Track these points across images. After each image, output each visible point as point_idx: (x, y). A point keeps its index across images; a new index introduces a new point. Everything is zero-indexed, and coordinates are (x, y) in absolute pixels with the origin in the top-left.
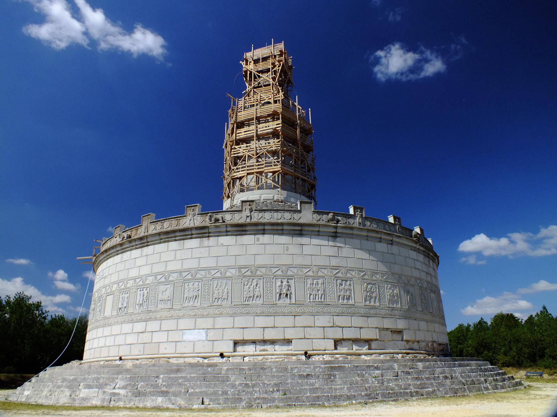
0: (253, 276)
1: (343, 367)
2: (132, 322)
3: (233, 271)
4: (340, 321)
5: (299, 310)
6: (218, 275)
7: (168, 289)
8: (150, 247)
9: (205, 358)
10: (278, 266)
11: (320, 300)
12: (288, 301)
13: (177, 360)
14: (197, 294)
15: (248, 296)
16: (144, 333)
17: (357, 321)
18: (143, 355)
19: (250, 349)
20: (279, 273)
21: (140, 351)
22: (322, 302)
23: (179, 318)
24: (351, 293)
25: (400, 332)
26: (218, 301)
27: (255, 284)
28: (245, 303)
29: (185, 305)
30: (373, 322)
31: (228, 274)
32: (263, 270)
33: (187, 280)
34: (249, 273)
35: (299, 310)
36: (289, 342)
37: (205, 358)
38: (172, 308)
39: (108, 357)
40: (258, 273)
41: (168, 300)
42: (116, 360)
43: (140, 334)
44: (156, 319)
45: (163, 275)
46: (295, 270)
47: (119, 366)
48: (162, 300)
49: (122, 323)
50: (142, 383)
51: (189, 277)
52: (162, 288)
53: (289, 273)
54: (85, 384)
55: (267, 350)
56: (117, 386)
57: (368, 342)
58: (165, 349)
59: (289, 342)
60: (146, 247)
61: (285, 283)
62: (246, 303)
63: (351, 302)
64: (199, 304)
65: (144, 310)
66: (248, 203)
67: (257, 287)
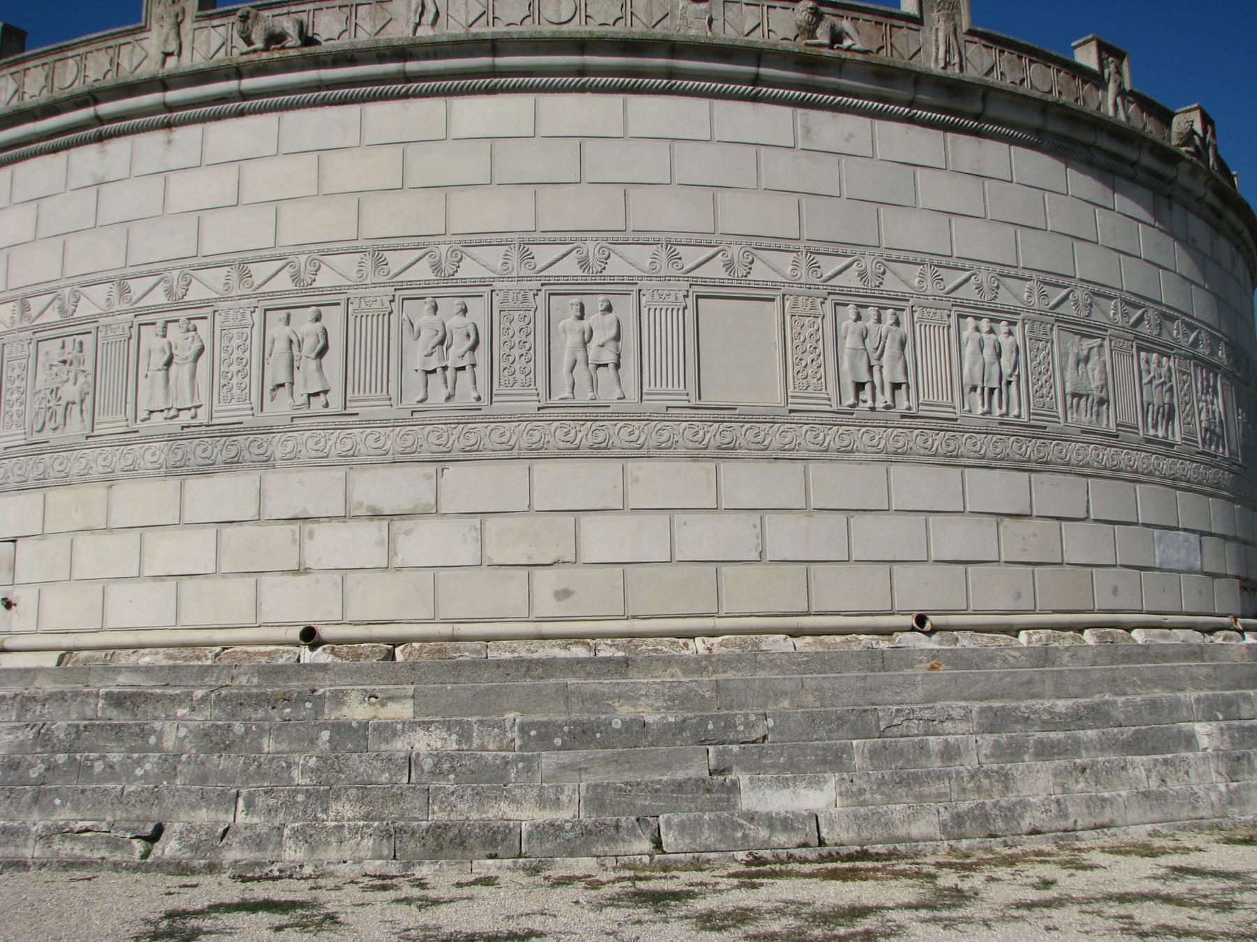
2: (957, 461)
7: (1094, 359)
8: (988, 143)
13: (1163, 636)
16: (1025, 520)
18: (1033, 612)
21: (1019, 595)
38: (1117, 436)
39: (808, 614)
41: (1102, 402)
42: (887, 632)
43: (1007, 521)
44: (1065, 468)
47: (1202, 653)
48: (1080, 396)
49: (890, 457)
54: (1230, 728)
58: (1115, 591)
60: (968, 137)
64: (1178, 438)
65: (1011, 418)
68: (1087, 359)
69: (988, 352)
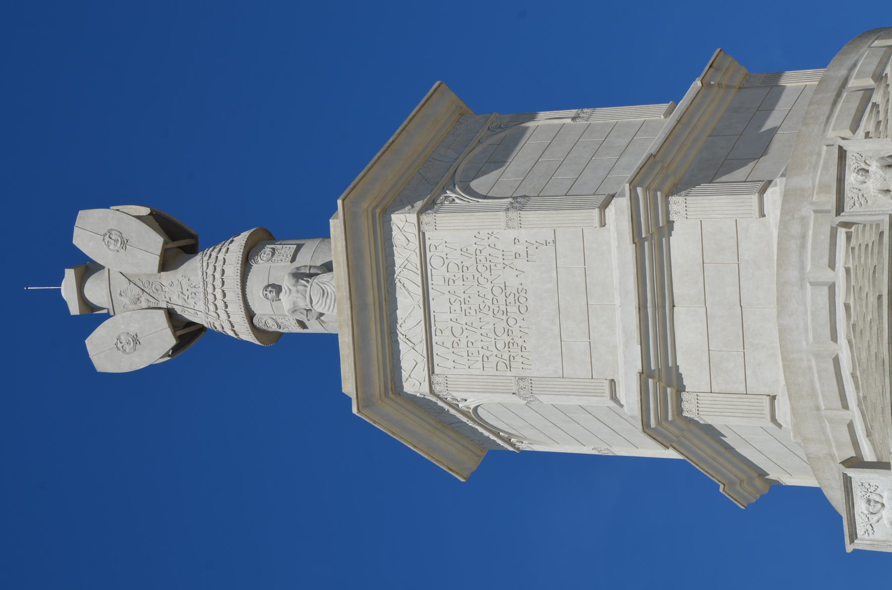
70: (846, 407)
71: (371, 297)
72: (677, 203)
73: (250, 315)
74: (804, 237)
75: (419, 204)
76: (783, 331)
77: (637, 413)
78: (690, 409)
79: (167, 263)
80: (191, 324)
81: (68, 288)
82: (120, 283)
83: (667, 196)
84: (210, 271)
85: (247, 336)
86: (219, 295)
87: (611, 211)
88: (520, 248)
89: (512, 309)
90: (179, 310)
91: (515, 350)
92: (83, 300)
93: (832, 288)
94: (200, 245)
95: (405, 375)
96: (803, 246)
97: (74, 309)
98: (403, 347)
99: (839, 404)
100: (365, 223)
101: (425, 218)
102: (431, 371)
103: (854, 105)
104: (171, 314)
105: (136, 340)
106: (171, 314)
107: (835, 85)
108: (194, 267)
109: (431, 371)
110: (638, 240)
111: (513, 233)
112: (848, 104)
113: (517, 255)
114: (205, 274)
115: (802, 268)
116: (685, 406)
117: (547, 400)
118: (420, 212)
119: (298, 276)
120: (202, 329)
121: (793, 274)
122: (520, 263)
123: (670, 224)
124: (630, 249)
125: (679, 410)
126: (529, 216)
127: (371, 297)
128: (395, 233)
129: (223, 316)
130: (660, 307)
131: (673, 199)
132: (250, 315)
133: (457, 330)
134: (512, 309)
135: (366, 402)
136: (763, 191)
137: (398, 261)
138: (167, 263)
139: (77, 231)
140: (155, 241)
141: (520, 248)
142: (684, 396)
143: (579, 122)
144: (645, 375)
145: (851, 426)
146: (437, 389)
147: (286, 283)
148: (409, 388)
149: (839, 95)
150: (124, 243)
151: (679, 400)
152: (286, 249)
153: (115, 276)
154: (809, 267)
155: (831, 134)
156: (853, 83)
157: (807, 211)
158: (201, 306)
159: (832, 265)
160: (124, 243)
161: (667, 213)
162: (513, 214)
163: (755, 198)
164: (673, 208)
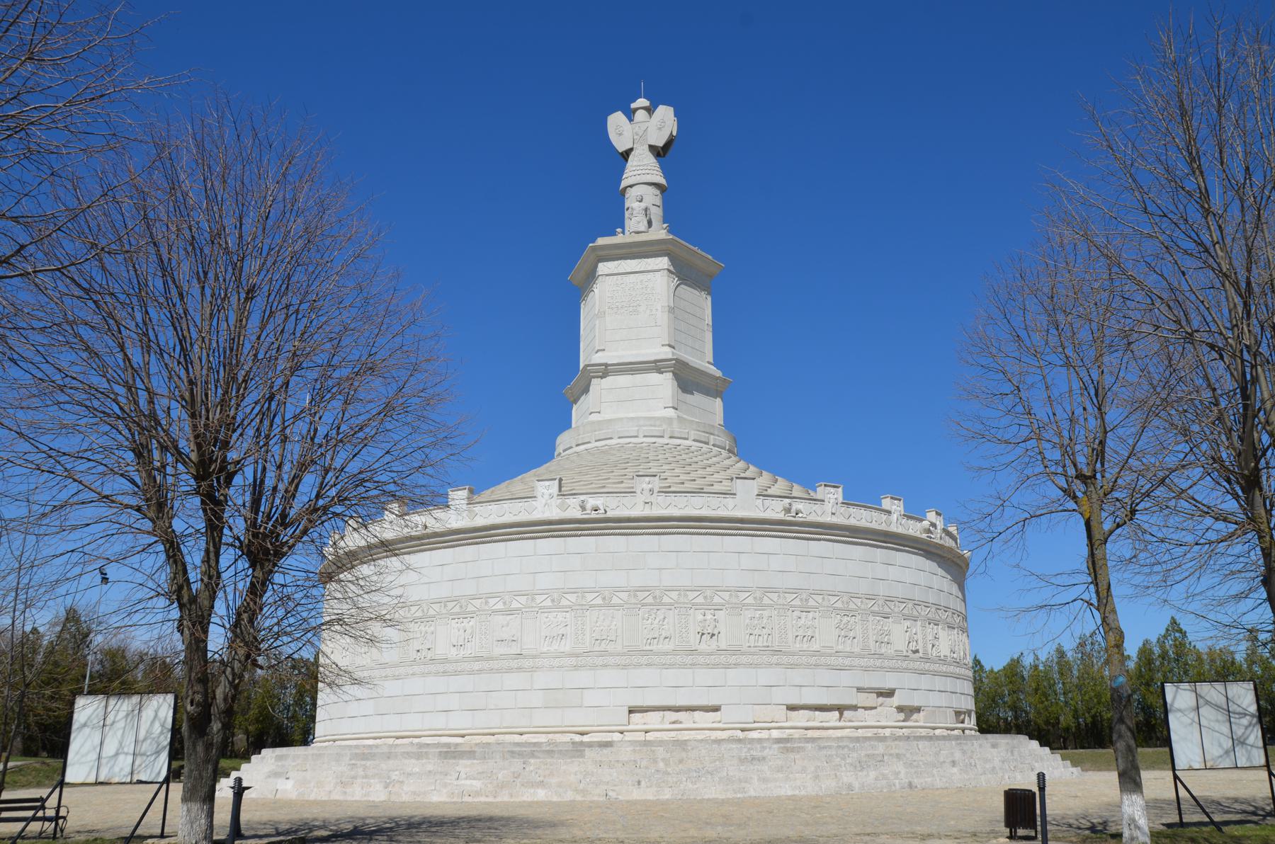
0: (658, 603)
1: (803, 747)
3: (624, 596)
4: (796, 676)
5: (732, 660)
6: (599, 601)
9: (582, 734)
10: (699, 589)
11: (765, 644)
12: (713, 644)
14: (564, 633)
15: (650, 637)
17: (825, 677)
19: (653, 719)
20: (700, 600)
22: (768, 647)
23: (534, 669)
24: (814, 632)
25: (890, 693)
26: (600, 644)
27: (662, 617)
28: (645, 648)
29: (545, 650)
30: (847, 679)
31: (615, 600)
32: (674, 595)
33: (544, 607)
34: (650, 600)
35: (732, 660)
36: (716, 709)
37: (582, 734)
40: (666, 600)
45: (499, 599)
46: (726, 595)
50: (506, 771)
51: (548, 603)
52: (500, 619)
53: (717, 600)
55: (681, 723)
56: (463, 775)
57: (841, 709)
59: (716, 709)
61: (709, 617)
62: (648, 648)
63: (815, 646)
66: (647, 479)
67: (665, 623)
68: (508, 625)
69: (462, 631)
70: (596, 441)
71: (634, 250)
72: (670, 375)
73: (631, 186)
74: (655, 426)
75: (672, 268)
76: (621, 419)
77: (592, 362)
78: (594, 381)
79: (652, 148)
80: (628, 157)
81: (642, 102)
82: (643, 127)
83: (673, 372)
84: (649, 168)
85: (623, 184)
86: (639, 172)
87: (668, 349)
88: (654, 312)
89: (631, 309)
90: (633, 153)
91: (615, 310)
92: (637, 109)
93: (636, 437)
94: (660, 158)
95: (605, 263)
96: (651, 426)
97: (633, 106)
98: (616, 262)
99: (597, 438)
100: (664, 247)
101: (666, 271)
102: (607, 275)
103: (703, 439)
104: (631, 150)
105: (620, 134)
106: (631, 150)
107: (712, 431)
108: (651, 160)
109: (607, 275)
110: (656, 361)
111: (659, 309)
112: (703, 436)
113: (651, 310)
114: (647, 165)
115: (644, 426)
116: (596, 380)
117: (597, 322)
118: (668, 270)
119: (646, 210)
120: (627, 161)
121: (642, 422)
122: (648, 311)
123: (662, 373)
124: (652, 358)
125: (594, 377)
126: (666, 316)
127: (634, 250)
128: (660, 259)
129: (631, 174)
130: (631, 370)
131: (671, 374)
132: (631, 186)
133: (623, 286)
134: (631, 309)
135: (594, 249)
136: (674, 408)
137: (649, 260)
138: (652, 148)
139: (665, 107)
140: (660, 143)
141: (654, 312)
142: (599, 379)
143: (706, 327)
144: (606, 365)
145: (589, 442)
146: (600, 278)
147: (643, 205)
148: (600, 265)
149: (707, 433)
150: (660, 129)
151: (598, 377)
152: (658, 201)
153: (647, 124)
154: (644, 428)
155: (693, 432)
156: (712, 437)
157: (664, 427)
158: (635, 163)
159: (645, 436)
160: (660, 129)
161: (666, 372)
162: (667, 309)
163: (671, 405)
164: (668, 374)
